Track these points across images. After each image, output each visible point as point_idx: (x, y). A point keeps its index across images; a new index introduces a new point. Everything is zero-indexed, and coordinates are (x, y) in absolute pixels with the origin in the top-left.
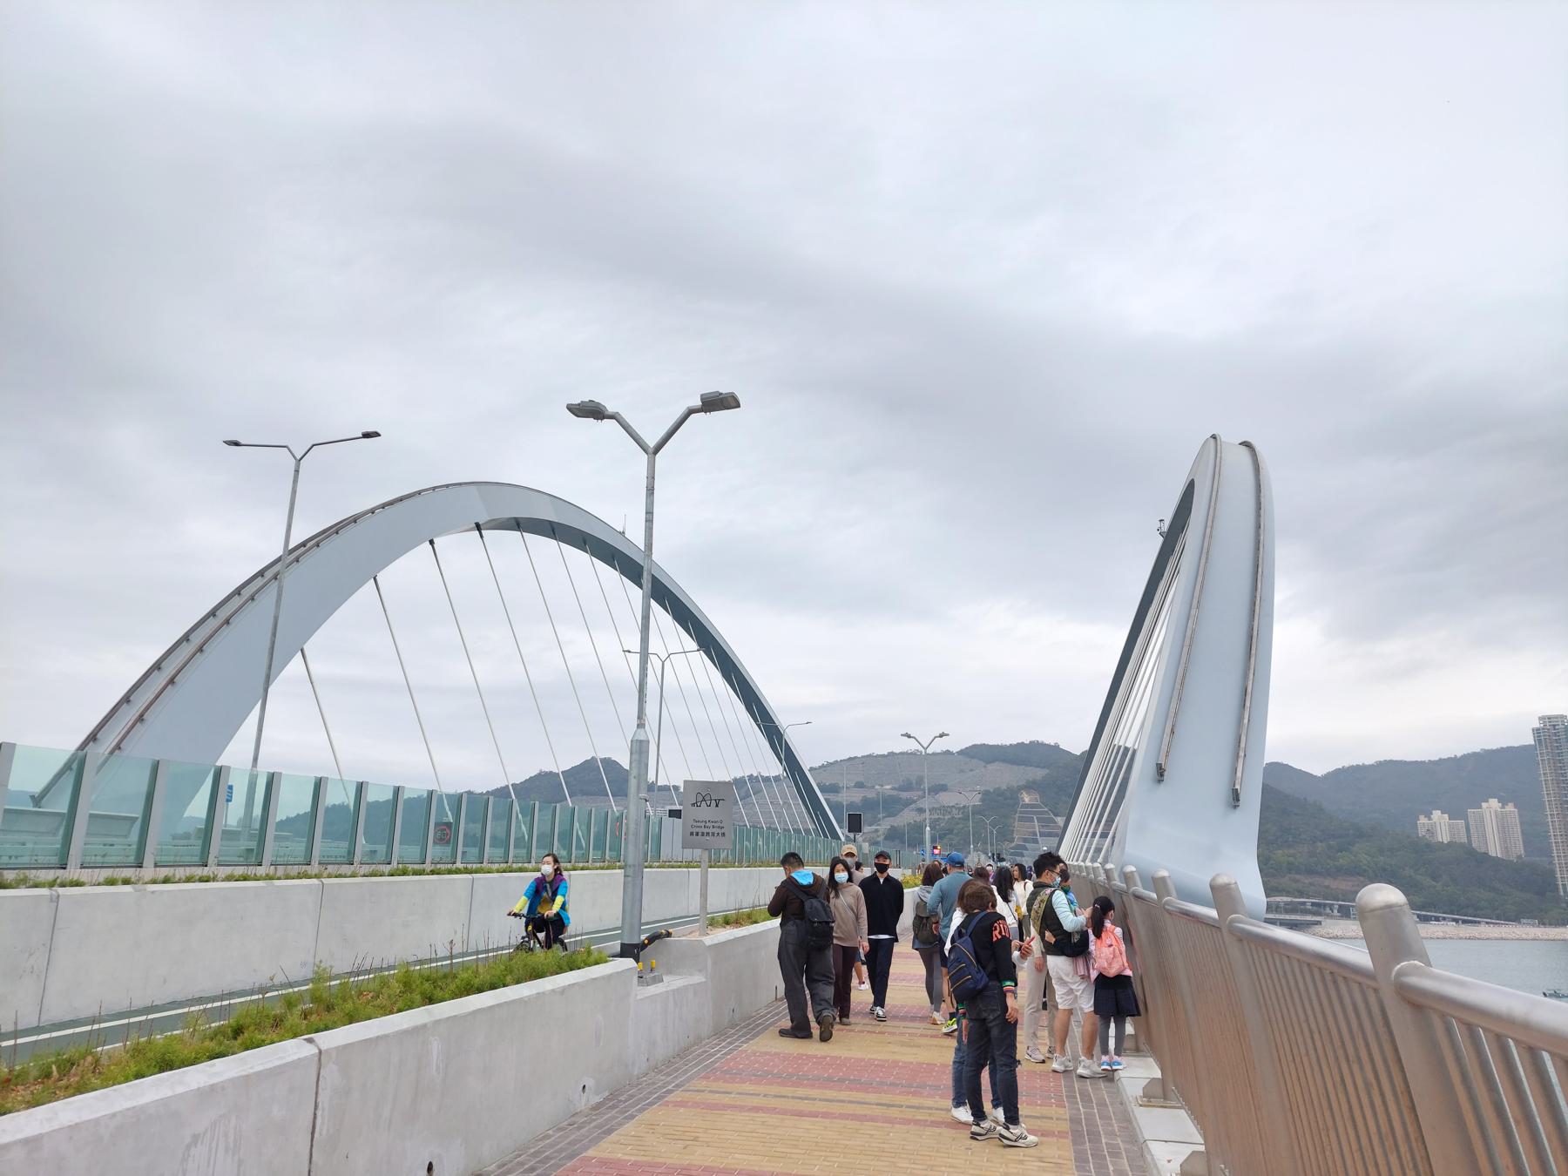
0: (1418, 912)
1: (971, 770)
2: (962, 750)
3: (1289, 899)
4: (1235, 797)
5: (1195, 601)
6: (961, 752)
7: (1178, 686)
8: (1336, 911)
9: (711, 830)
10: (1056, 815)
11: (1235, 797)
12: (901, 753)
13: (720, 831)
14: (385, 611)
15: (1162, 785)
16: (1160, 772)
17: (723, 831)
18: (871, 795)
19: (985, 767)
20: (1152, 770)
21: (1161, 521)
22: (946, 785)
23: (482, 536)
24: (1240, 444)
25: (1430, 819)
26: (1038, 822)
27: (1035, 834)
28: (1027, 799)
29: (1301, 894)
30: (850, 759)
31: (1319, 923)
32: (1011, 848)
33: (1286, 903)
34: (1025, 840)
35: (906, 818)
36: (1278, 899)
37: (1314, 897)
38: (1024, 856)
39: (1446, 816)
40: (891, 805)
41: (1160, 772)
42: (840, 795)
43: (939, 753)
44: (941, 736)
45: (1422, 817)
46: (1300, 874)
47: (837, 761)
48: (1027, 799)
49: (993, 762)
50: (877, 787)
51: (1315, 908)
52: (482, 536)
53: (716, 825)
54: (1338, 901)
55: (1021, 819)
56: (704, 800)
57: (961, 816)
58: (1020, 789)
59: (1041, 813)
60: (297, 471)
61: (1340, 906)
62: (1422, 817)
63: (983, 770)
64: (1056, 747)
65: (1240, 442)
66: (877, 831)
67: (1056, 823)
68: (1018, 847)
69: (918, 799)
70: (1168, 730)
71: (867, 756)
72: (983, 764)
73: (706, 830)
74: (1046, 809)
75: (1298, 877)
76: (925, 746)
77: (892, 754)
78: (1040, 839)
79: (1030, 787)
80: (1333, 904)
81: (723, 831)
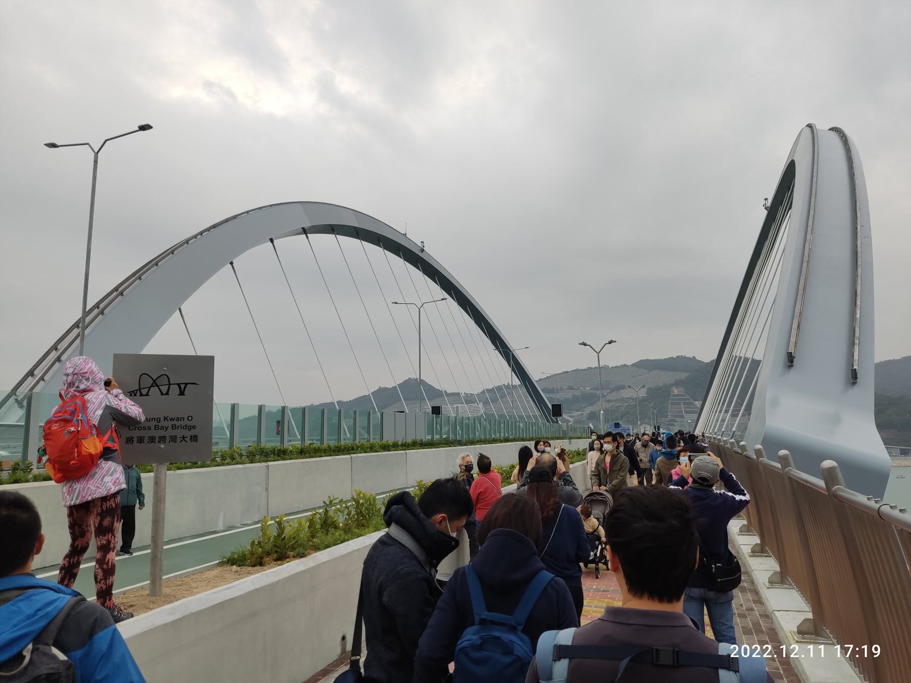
1: (640, 376)
2: (633, 364)
4: (854, 377)
5: (810, 228)
6: (633, 365)
7: (801, 292)
9: (170, 432)
11: (854, 377)
13: (188, 434)
14: (240, 286)
15: (792, 370)
16: (790, 359)
17: (193, 432)
18: (577, 393)
19: (648, 373)
20: (782, 357)
21: (766, 199)
23: (307, 237)
24: (830, 129)
26: (684, 405)
27: (681, 412)
28: (676, 392)
30: (564, 373)
32: (667, 421)
34: (675, 416)
38: (674, 426)
40: (590, 399)
41: (790, 359)
44: (610, 343)
48: (676, 391)
49: (652, 370)
52: (307, 237)
53: (178, 423)
55: (672, 404)
56: (155, 383)
58: (671, 385)
59: (685, 399)
60: (96, 162)
63: (647, 375)
64: (694, 358)
65: (828, 128)
66: (582, 414)
67: (694, 404)
68: (670, 420)
69: (607, 395)
70: (795, 326)
72: (646, 371)
73: (161, 433)
74: (688, 397)
76: (598, 352)
77: (590, 368)
79: (677, 384)
81: (193, 432)
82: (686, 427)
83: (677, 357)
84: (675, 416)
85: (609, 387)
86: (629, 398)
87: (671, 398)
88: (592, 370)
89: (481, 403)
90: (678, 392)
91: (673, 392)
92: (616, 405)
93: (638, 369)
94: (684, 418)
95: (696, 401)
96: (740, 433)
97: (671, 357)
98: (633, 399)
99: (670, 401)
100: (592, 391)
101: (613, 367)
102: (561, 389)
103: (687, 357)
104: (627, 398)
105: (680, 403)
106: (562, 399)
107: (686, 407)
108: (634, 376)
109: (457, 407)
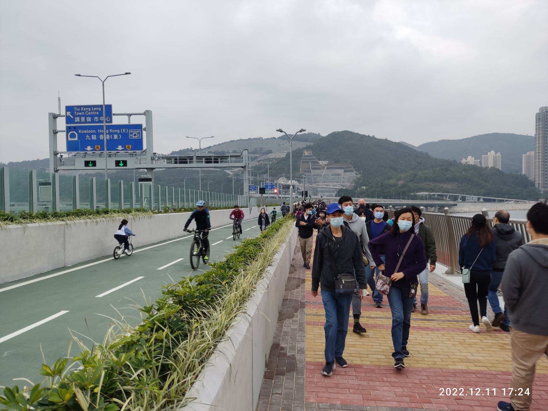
0: (483, 197)
1: (283, 145)
3: (428, 193)
8: (448, 198)
10: (319, 160)
12: (254, 139)
22: (272, 150)
25: (467, 160)
26: (311, 163)
27: (309, 168)
28: (306, 153)
29: (433, 191)
31: (456, 205)
32: (298, 175)
33: (426, 195)
36: (422, 193)
37: (439, 192)
39: (473, 158)
45: (464, 159)
46: (430, 182)
48: (306, 153)
51: (439, 197)
54: (449, 193)
55: (303, 162)
57: (277, 162)
58: (304, 149)
61: (450, 195)
62: (464, 159)
63: (288, 144)
64: (319, 134)
67: (318, 163)
74: (315, 158)
75: (429, 183)
79: (307, 148)
80: (447, 195)
82: (312, 179)
84: (305, 171)
86: (273, 158)
87: (303, 158)
90: (308, 154)
91: (305, 154)
93: (282, 140)
94: (311, 172)
98: (276, 159)
99: (302, 160)
101: (265, 139)
105: (309, 161)
108: (279, 145)
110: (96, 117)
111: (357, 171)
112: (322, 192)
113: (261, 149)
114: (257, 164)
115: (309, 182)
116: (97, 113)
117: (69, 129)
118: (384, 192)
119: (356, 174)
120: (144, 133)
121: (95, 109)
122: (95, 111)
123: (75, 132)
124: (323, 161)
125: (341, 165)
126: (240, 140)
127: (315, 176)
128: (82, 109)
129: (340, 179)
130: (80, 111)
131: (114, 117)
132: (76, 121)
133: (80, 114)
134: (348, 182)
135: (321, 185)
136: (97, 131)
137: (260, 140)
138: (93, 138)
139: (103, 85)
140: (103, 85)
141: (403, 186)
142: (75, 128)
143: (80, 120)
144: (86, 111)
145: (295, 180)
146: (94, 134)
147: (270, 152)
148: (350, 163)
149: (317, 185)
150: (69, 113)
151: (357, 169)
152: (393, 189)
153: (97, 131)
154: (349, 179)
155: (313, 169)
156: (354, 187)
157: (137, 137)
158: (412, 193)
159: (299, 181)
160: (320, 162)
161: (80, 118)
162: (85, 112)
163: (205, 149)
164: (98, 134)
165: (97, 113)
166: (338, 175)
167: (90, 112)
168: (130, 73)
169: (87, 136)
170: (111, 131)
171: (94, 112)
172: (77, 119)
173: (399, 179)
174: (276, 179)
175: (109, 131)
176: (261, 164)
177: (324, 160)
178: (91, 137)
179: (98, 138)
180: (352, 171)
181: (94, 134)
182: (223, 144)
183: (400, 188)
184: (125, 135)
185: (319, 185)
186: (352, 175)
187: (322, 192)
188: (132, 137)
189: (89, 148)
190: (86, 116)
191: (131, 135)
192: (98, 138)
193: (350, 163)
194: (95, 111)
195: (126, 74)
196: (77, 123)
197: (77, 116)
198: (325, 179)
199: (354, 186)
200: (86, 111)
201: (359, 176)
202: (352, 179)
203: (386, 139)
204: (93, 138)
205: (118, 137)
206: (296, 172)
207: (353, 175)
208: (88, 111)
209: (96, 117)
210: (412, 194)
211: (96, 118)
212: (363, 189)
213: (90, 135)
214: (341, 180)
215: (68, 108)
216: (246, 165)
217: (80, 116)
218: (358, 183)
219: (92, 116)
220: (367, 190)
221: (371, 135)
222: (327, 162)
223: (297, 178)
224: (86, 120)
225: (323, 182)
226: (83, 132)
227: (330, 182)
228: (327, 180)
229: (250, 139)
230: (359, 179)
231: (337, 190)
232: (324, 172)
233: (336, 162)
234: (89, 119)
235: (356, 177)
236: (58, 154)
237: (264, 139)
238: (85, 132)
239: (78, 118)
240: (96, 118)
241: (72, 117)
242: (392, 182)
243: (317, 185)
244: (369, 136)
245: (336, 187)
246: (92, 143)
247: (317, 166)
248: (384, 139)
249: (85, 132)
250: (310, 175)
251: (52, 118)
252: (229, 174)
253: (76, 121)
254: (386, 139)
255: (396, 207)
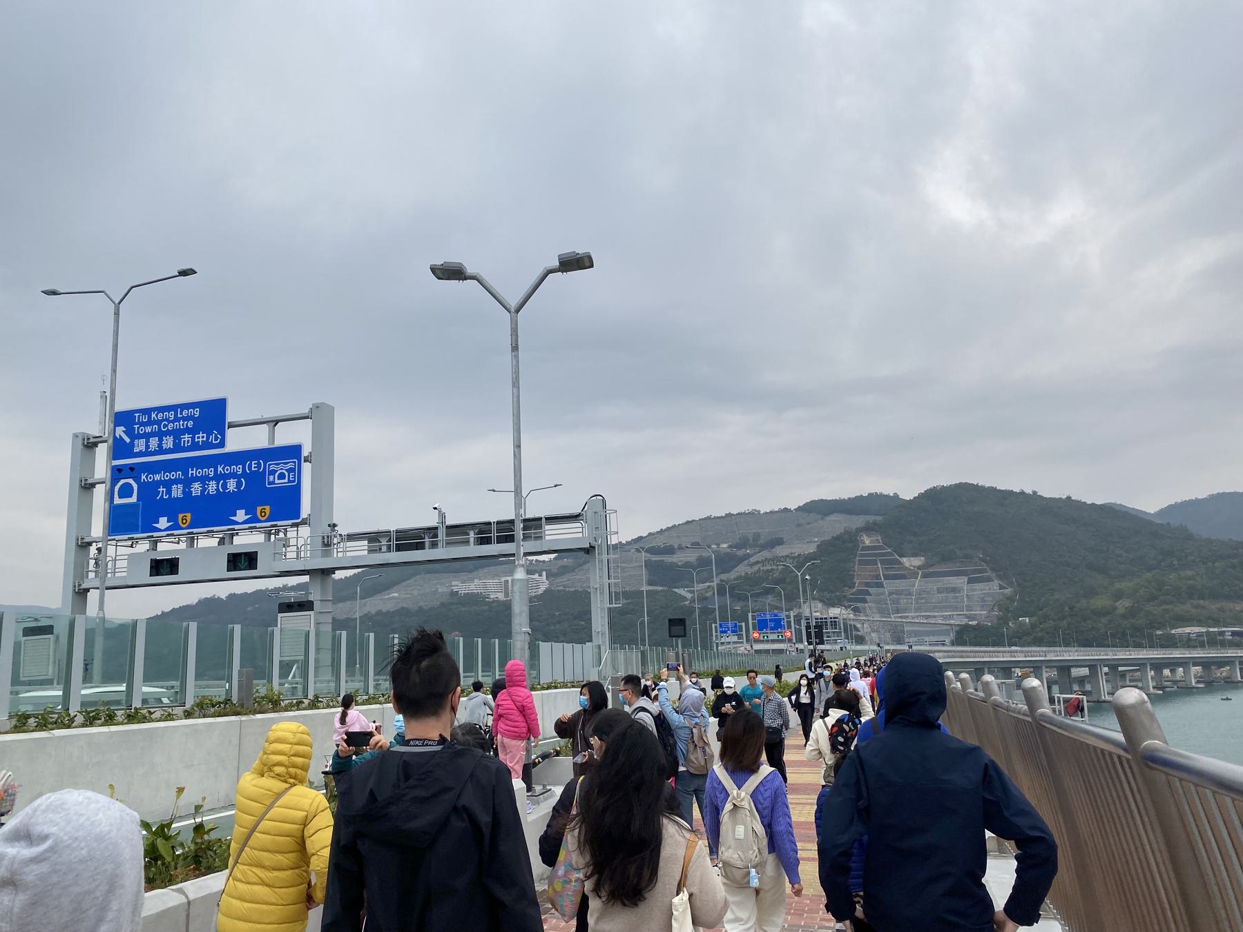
1: (809, 524)
6: (799, 509)
10: (902, 556)
12: (738, 514)
22: (782, 539)
27: (878, 577)
32: (853, 594)
34: (868, 585)
35: (742, 569)
42: (675, 556)
43: (776, 511)
47: (675, 525)
50: (713, 546)
55: (861, 563)
58: (860, 530)
59: (883, 555)
64: (896, 496)
67: (900, 563)
68: (860, 592)
71: (705, 518)
72: (820, 516)
74: (890, 550)
78: (885, 583)
79: (868, 529)
83: (870, 495)
84: (868, 585)
85: (759, 543)
86: (787, 556)
88: (733, 517)
89: (544, 573)
90: (870, 542)
91: (864, 543)
92: (765, 568)
94: (883, 587)
95: (905, 557)
96: (985, 612)
97: (859, 495)
98: (794, 558)
99: (857, 558)
100: (729, 550)
101: (766, 513)
102: (681, 548)
103: (884, 495)
104: (783, 556)
105: (876, 560)
106: (679, 564)
107: (886, 568)
108: (799, 525)
109: (507, 582)
110: (187, 436)
111: (1000, 577)
112: (911, 634)
113: (757, 536)
114: (750, 571)
115: (882, 612)
116: (190, 424)
117: (117, 473)
118: (1082, 629)
119: (1001, 587)
120: (307, 468)
121: (185, 413)
122: (184, 419)
123: (131, 481)
124: (912, 559)
125: (958, 564)
126: (708, 518)
127: (895, 596)
128: (153, 415)
129: (959, 600)
130: (150, 423)
131: (230, 433)
132: (136, 450)
133: (148, 429)
134: (982, 606)
135: (913, 618)
136: (185, 473)
137: (753, 514)
138: (174, 494)
139: (117, 314)
140: (117, 314)
141: (1131, 613)
142: (132, 468)
143: (147, 446)
144: (163, 420)
145: (845, 607)
146: (176, 481)
147: (779, 542)
148: (981, 559)
149: (901, 617)
150: (120, 431)
151: (1001, 573)
152: (1104, 620)
153: (185, 473)
154: (983, 600)
155: (887, 577)
156: (999, 619)
157: (286, 480)
158: (1159, 629)
159: (856, 610)
160: (905, 561)
161: (147, 442)
162: (158, 422)
163: (628, 543)
164: (187, 482)
165: (190, 424)
166: (954, 590)
167: (173, 422)
168: (192, 272)
169: (161, 490)
170: (220, 469)
171: (181, 423)
172: (140, 445)
173: (1119, 595)
174: (796, 606)
175: (216, 470)
176: (759, 571)
177: (915, 555)
178: (169, 492)
179: (187, 493)
180: (989, 580)
181: (176, 481)
182: (668, 529)
183: (1124, 616)
184: (256, 479)
185: (908, 617)
186: (990, 589)
187: (911, 634)
188: (273, 483)
189: (163, 523)
190: (160, 435)
191: (271, 478)
192: (187, 493)
193: (981, 559)
194: (184, 419)
195: (184, 273)
196: (140, 454)
197: (140, 436)
198: (923, 601)
199: (999, 618)
200: (163, 420)
201: (1008, 591)
202: (990, 599)
203: (1069, 498)
204: (174, 494)
205: (239, 484)
206: (844, 586)
207: (993, 588)
208: (167, 420)
209: (187, 436)
210: (1159, 632)
211: (186, 438)
212: (1022, 624)
213: (168, 485)
214: (963, 602)
215: (123, 418)
216: (594, 543)
217: (147, 436)
218: (1007, 610)
219: (177, 434)
220: (1033, 626)
221: (1029, 491)
222: (922, 558)
223: (850, 600)
224: (160, 446)
225: (917, 610)
226: (151, 478)
227: (934, 609)
228: (927, 602)
229: (729, 515)
230: (1010, 599)
231: (957, 628)
232: (918, 584)
233: (945, 558)
234: (169, 442)
235: (1003, 593)
236: (90, 544)
237: (762, 512)
238: (157, 477)
239: (143, 441)
240: (186, 438)
241: (128, 440)
242: (1101, 602)
243: (901, 617)
244: (1022, 493)
245: (952, 622)
246: (171, 509)
247: (899, 569)
248: (1064, 497)
249: (157, 477)
250: (883, 594)
251: (80, 446)
252: (685, 599)
253: (136, 450)
254: (1069, 498)
255: (1120, 669)
